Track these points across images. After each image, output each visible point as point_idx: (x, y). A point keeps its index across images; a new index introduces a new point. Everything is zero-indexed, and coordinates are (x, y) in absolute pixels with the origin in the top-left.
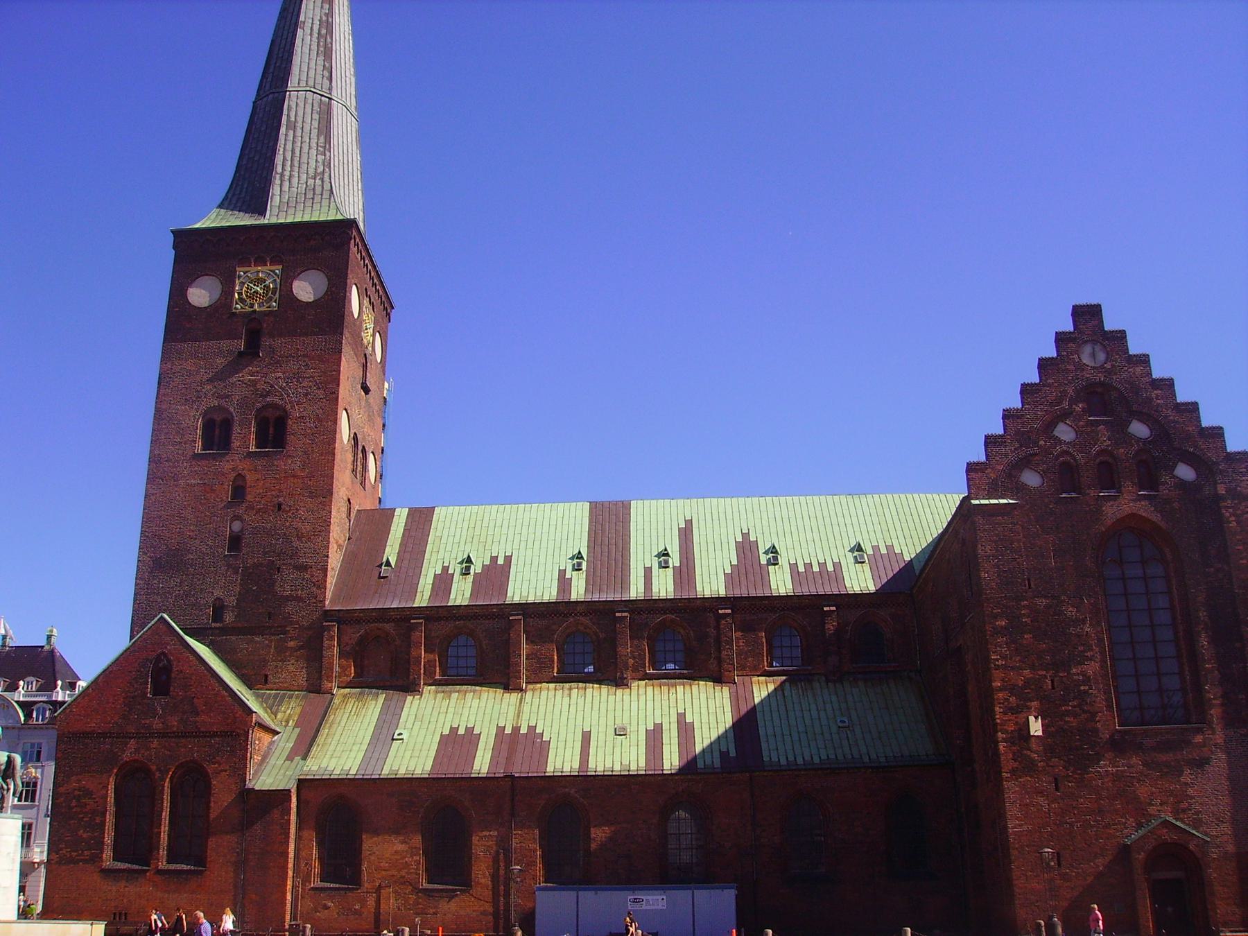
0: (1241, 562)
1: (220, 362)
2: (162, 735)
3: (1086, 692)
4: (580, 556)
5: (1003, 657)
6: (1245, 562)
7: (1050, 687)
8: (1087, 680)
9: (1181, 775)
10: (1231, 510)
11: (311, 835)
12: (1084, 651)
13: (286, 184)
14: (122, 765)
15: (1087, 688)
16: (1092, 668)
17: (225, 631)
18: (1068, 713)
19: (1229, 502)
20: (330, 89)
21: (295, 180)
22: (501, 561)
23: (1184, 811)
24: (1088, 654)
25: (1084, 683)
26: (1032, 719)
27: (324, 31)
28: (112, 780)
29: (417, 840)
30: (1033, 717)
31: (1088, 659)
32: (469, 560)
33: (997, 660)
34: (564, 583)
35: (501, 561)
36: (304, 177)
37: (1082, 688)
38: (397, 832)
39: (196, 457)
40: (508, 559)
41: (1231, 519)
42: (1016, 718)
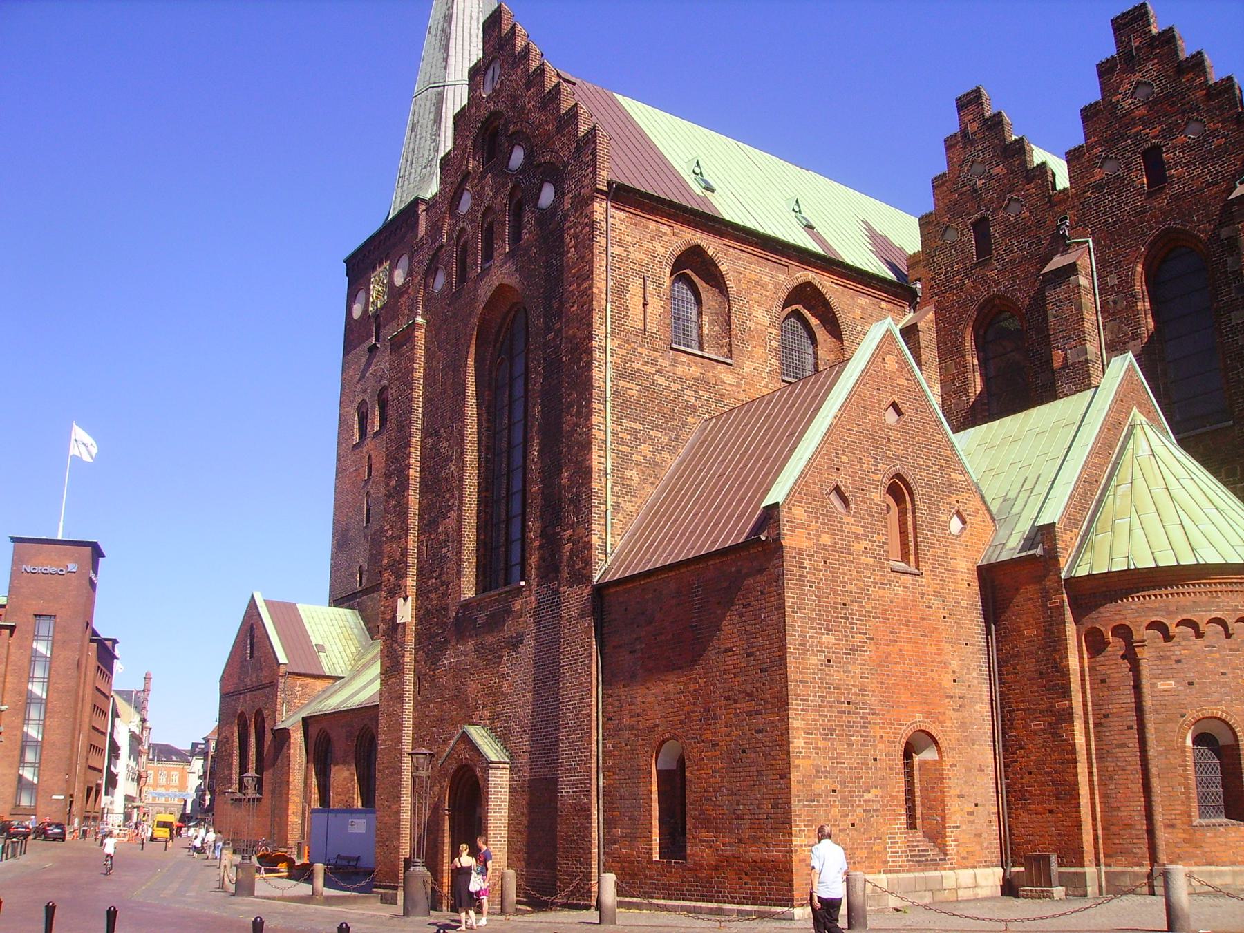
1: (364, 360)
2: (252, 689)
9: (500, 663)
11: (312, 766)
13: (406, 182)
14: (239, 716)
17: (365, 592)
20: (445, 77)
21: (413, 176)
26: (401, 601)
27: (446, 25)
28: (236, 729)
29: (353, 768)
30: (402, 599)
38: (345, 762)
39: (355, 447)
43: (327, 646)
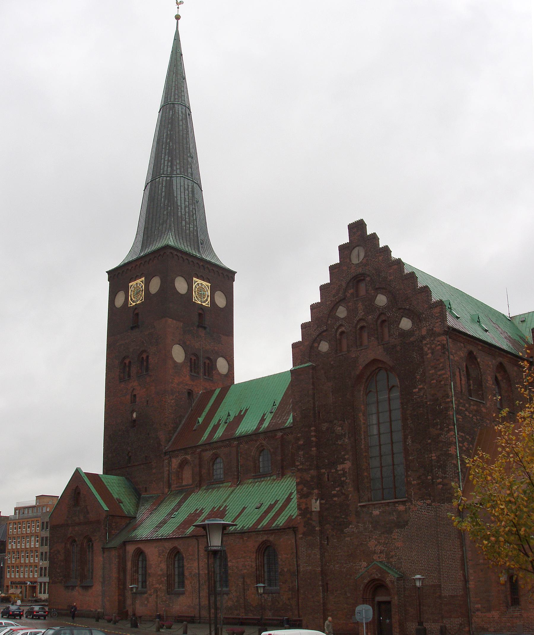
0: (432, 382)
3: (344, 481)
4: (275, 404)
5: (302, 464)
6: (435, 381)
7: (327, 480)
8: (344, 474)
10: (428, 346)
12: (344, 455)
15: (345, 478)
16: (348, 465)
18: (335, 495)
19: (428, 340)
22: (242, 414)
23: (392, 557)
24: (347, 457)
25: (344, 475)
31: (345, 459)
32: (229, 415)
33: (298, 466)
34: (263, 420)
35: (242, 414)
36: (158, 225)
37: (342, 479)
40: (246, 410)
41: (428, 352)
42: (306, 500)
43: (123, 500)
